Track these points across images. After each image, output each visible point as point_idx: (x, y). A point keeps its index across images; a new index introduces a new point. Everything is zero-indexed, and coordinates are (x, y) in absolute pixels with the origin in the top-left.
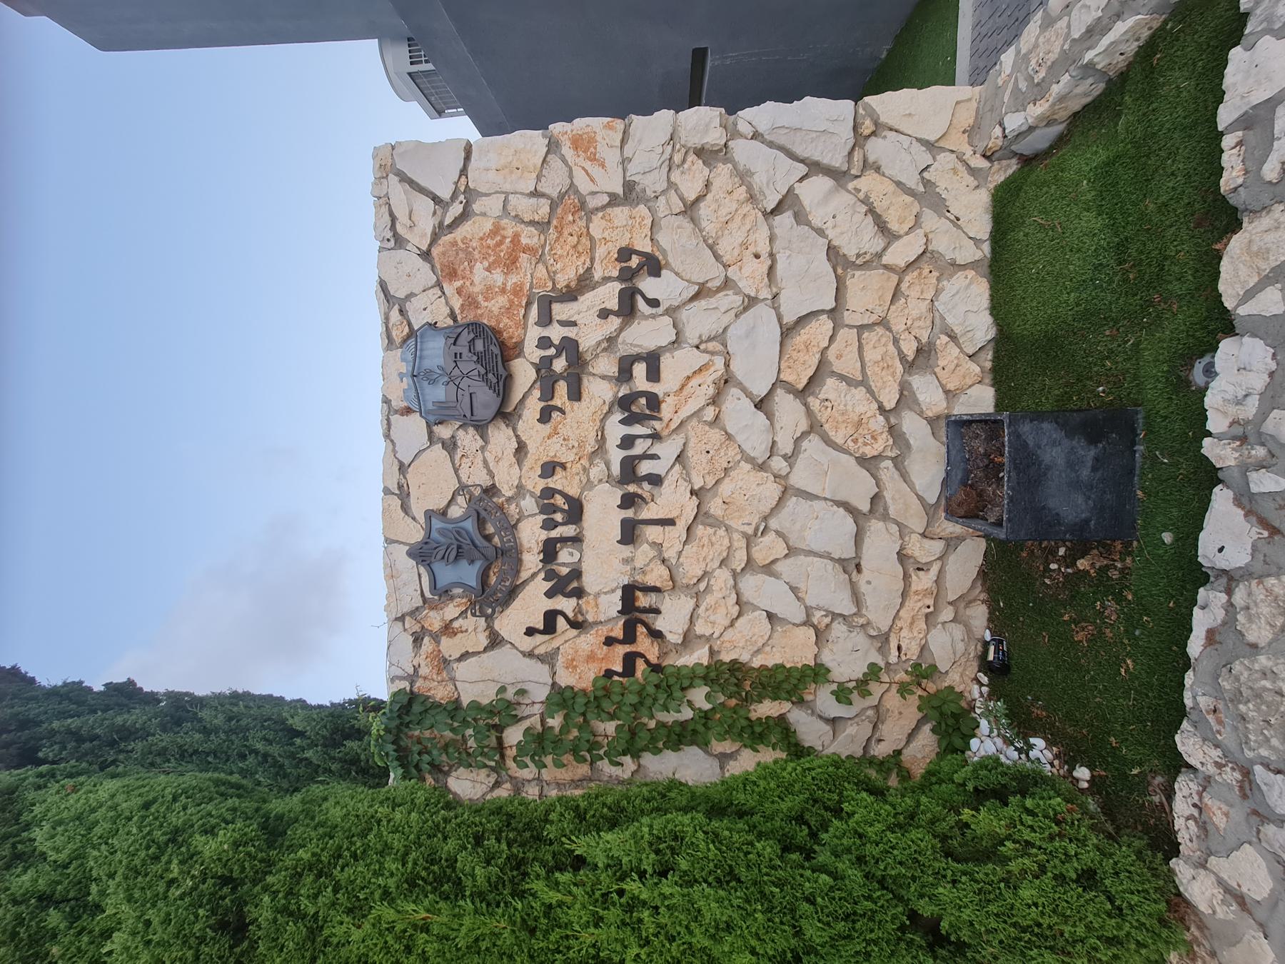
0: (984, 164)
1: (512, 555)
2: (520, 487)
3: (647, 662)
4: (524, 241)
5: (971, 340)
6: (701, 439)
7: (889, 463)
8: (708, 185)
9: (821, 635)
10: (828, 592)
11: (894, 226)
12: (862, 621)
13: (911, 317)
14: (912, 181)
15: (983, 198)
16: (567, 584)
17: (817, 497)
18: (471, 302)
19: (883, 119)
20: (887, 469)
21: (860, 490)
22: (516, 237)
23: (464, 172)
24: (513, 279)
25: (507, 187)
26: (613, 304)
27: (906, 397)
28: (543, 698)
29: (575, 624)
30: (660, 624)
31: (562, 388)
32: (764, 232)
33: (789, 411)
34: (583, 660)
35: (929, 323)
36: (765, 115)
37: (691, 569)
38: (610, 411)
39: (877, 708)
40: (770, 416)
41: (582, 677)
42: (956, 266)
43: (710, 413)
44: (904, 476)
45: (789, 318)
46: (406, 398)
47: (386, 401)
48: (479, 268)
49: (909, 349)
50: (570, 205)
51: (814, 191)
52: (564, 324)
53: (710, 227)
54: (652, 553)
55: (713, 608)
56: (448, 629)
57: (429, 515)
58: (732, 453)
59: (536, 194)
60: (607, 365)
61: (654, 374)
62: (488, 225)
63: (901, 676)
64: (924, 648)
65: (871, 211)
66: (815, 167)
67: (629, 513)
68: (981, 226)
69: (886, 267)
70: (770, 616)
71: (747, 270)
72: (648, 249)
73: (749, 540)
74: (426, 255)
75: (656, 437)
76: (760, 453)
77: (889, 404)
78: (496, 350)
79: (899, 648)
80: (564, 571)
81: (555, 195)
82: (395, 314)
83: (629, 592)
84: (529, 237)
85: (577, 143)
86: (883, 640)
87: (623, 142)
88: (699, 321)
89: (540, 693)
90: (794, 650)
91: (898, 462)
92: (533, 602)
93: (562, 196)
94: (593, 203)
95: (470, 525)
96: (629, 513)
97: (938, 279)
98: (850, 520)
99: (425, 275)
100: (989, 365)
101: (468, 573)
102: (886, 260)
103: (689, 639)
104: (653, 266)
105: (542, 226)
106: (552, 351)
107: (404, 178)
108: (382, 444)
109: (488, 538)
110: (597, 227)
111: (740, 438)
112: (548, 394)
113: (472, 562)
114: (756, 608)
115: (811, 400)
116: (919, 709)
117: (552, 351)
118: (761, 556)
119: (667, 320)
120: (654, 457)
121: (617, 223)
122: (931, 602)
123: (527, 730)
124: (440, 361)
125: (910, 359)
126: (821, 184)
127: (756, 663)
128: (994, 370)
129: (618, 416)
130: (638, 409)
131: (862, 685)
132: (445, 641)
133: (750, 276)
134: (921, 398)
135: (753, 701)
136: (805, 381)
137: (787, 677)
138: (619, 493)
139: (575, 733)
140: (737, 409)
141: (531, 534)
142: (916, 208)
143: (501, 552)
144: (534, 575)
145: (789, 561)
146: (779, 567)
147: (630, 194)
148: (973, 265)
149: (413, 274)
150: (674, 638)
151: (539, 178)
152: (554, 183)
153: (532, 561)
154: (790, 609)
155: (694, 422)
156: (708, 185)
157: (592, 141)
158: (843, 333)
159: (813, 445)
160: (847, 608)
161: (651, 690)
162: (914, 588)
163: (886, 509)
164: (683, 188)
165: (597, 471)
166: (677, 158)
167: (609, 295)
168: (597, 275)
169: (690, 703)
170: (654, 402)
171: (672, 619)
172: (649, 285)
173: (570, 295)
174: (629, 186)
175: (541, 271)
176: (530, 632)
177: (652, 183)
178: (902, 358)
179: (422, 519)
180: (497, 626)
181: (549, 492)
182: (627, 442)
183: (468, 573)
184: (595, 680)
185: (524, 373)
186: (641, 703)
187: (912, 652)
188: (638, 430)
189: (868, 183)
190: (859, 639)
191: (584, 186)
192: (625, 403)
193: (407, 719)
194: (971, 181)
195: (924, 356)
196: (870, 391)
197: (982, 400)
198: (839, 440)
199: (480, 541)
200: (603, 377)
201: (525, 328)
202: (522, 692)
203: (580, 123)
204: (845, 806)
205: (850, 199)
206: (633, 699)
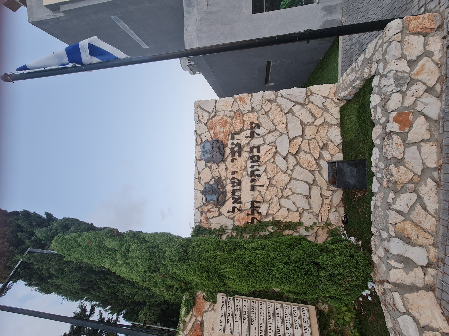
0: (338, 101)
1: (224, 193)
2: (226, 177)
3: (257, 220)
4: (228, 121)
5: (337, 142)
6: (270, 166)
7: (317, 172)
8: (271, 108)
9: (301, 214)
10: (302, 203)
11: (316, 116)
12: (311, 211)
14: (321, 105)
15: (338, 109)
16: (237, 200)
17: (299, 180)
18: (216, 135)
19: (313, 92)
20: (316, 173)
21: (310, 179)
23: (215, 106)
24: (225, 130)
25: (224, 109)
26: (249, 135)
27: (321, 156)
28: (231, 228)
29: (239, 210)
30: (260, 210)
31: (237, 154)
32: (285, 118)
33: (291, 160)
34: (241, 219)
35: (326, 138)
36: (285, 92)
37: (268, 197)
38: (248, 160)
39: (316, 233)
40: (287, 161)
41: (241, 223)
42: (332, 125)
44: (321, 175)
45: (291, 138)
46: (201, 157)
47: (196, 157)
49: (321, 144)
50: (239, 113)
51: (296, 109)
52: (237, 139)
53: (272, 117)
54: (258, 193)
55: (274, 207)
56: (209, 211)
57: (205, 183)
58: (278, 169)
59: (231, 111)
60: (247, 149)
61: (259, 151)
62: (220, 118)
63: (322, 225)
64: (328, 218)
65: (311, 112)
66: (296, 103)
67: (253, 184)
68: (338, 115)
69: (315, 125)
70: (288, 209)
71: (281, 127)
72: (257, 122)
73: (282, 191)
74: (206, 125)
75: (259, 165)
76: (284, 169)
77: (317, 158)
78: (222, 146)
79: (321, 218)
80: (237, 197)
81: (235, 111)
82: (198, 138)
83: (253, 202)
84: (229, 120)
85: (241, 99)
86: (317, 216)
87: (251, 99)
88: (270, 138)
89: (231, 227)
90: (294, 218)
91: (319, 172)
92: (229, 205)
93: (237, 111)
94: (244, 112)
95: (215, 186)
96: (253, 184)
97: (328, 128)
98: (307, 186)
99: (205, 129)
100: (341, 148)
101: (214, 197)
102: (314, 124)
103: (267, 215)
104: (258, 126)
105: (232, 118)
106: (235, 146)
108: (194, 167)
109: (219, 189)
110: (245, 118)
111: (279, 166)
112: (233, 155)
113: (215, 195)
114: (284, 207)
115: (297, 157)
116: (327, 233)
117: (235, 146)
118: (285, 194)
119: (262, 138)
120: (259, 170)
121: (250, 117)
122: (329, 206)
123: (228, 236)
124: (209, 148)
125: (321, 147)
126: (298, 107)
127: (285, 221)
128: (342, 149)
129: (250, 161)
130: (255, 159)
131: (312, 227)
132: (208, 214)
133: (281, 128)
134: (324, 156)
135: (284, 230)
136: (295, 152)
137: (292, 225)
138: (250, 179)
139: (239, 237)
140: (279, 159)
141: (229, 188)
142: (322, 111)
143: (222, 193)
144: (230, 198)
145: (293, 195)
146: (290, 197)
147: (253, 110)
148: (336, 125)
149: (203, 129)
150: (264, 214)
151: (232, 107)
152: (235, 109)
153: (229, 195)
154: (294, 208)
155: (268, 162)
156: (271, 108)
157: (244, 99)
158: (304, 141)
159: (298, 167)
160: (308, 208)
161: (258, 226)
162: (325, 203)
163: (317, 183)
164: (265, 109)
165: (245, 174)
166: (264, 102)
167: (248, 133)
168: (245, 128)
169: (268, 230)
170: (259, 157)
171: (263, 209)
172: (257, 131)
173: (239, 133)
174: (252, 109)
175: (232, 128)
176: (229, 212)
177: (258, 108)
178: (320, 147)
179: (204, 185)
180: (220, 210)
181: (233, 178)
182: (252, 167)
183: (214, 197)
184: (244, 224)
185: (228, 151)
186: (256, 230)
187: (325, 219)
188: (255, 164)
189: (310, 106)
190: (311, 215)
191: (242, 109)
192: (252, 158)
193: (199, 232)
194: (335, 106)
195: (325, 146)
196: (311, 154)
197: (340, 157)
198: (304, 166)
199: (217, 190)
200: (246, 152)
201: (228, 140)
202: (226, 227)
203: (241, 95)
204: (301, 243)
205: (305, 110)
206: (254, 228)
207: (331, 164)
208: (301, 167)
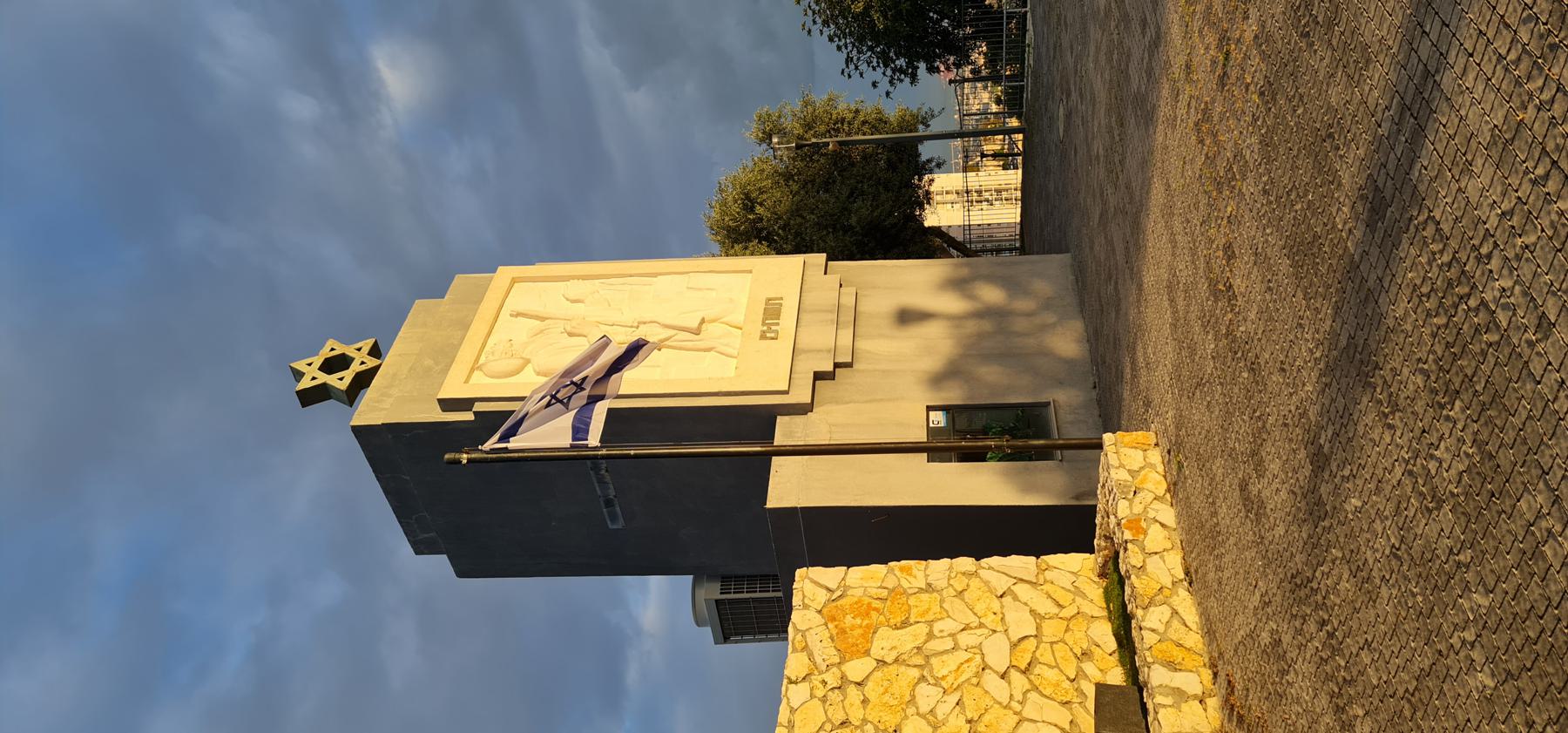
13: (1077, 639)
36: (995, 561)
43: (975, 681)
45: (1015, 639)
65: (1049, 596)
74: (820, 612)
82: (799, 637)
84: (876, 604)
88: (966, 639)
99: (818, 619)
110: (912, 601)
133: (989, 620)
140: (991, 681)
147: (929, 588)
157: (910, 568)
159: (1033, 696)
189: (1047, 587)
191: (905, 584)
198: (1046, 692)
207: (1101, 689)
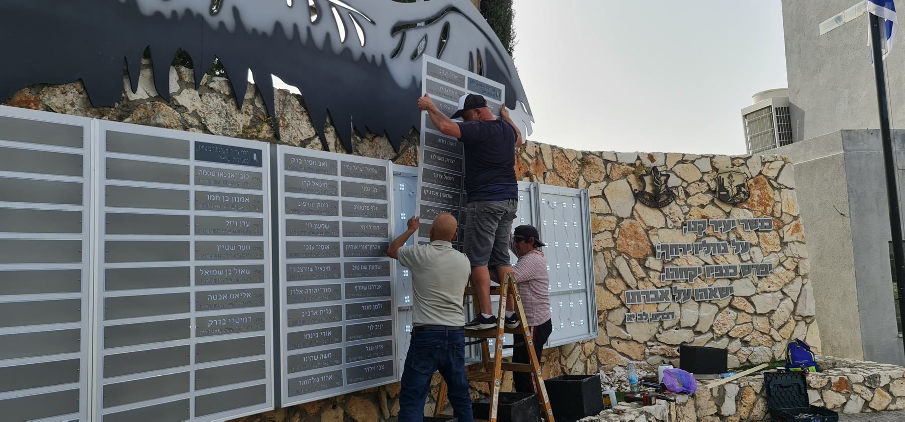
8: (788, 270)
11: (782, 331)
12: (661, 330)
19: (811, 325)
20: (710, 335)
22: (769, 205)
32: (776, 289)
45: (753, 299)
47: (714, 156)
48: (758, 192)
49: (747, 339)
51: (788, 303)
59: (782, 213)
62: (772, 196)
66: (796, 304)
74: (760, 173)
82: (742, 161)
84: (769, 210)
91: (712, 339)
94: (780, 231)
105: (772, 214)
107: (783, 166)
108: (698, 153)
110: (774, 233)
140: (724, 283)
147: (784, 244)
148: (774, 357)
152: (785, 218)
156: (788, 270)
157: (798, 231)
174: (786, 244)
177: (788, 252)
191: (786, 228)
195: (745, 343)
198: (718, 318)
208: (716, 315)
